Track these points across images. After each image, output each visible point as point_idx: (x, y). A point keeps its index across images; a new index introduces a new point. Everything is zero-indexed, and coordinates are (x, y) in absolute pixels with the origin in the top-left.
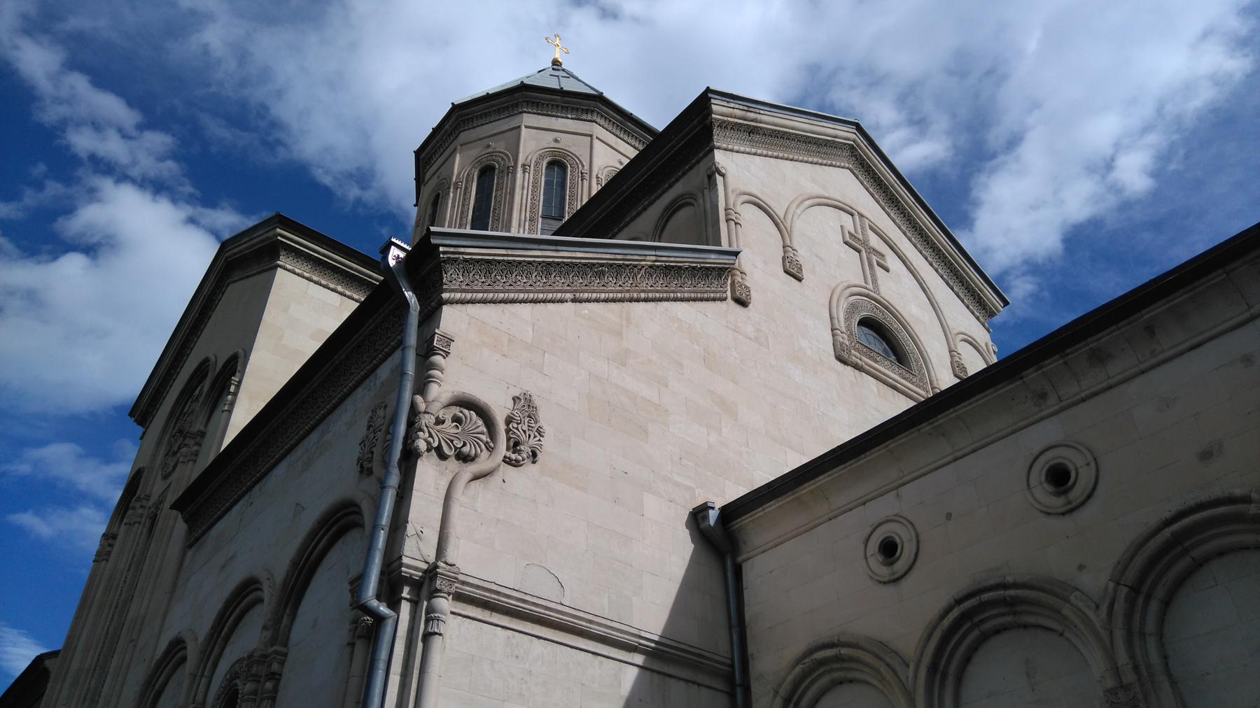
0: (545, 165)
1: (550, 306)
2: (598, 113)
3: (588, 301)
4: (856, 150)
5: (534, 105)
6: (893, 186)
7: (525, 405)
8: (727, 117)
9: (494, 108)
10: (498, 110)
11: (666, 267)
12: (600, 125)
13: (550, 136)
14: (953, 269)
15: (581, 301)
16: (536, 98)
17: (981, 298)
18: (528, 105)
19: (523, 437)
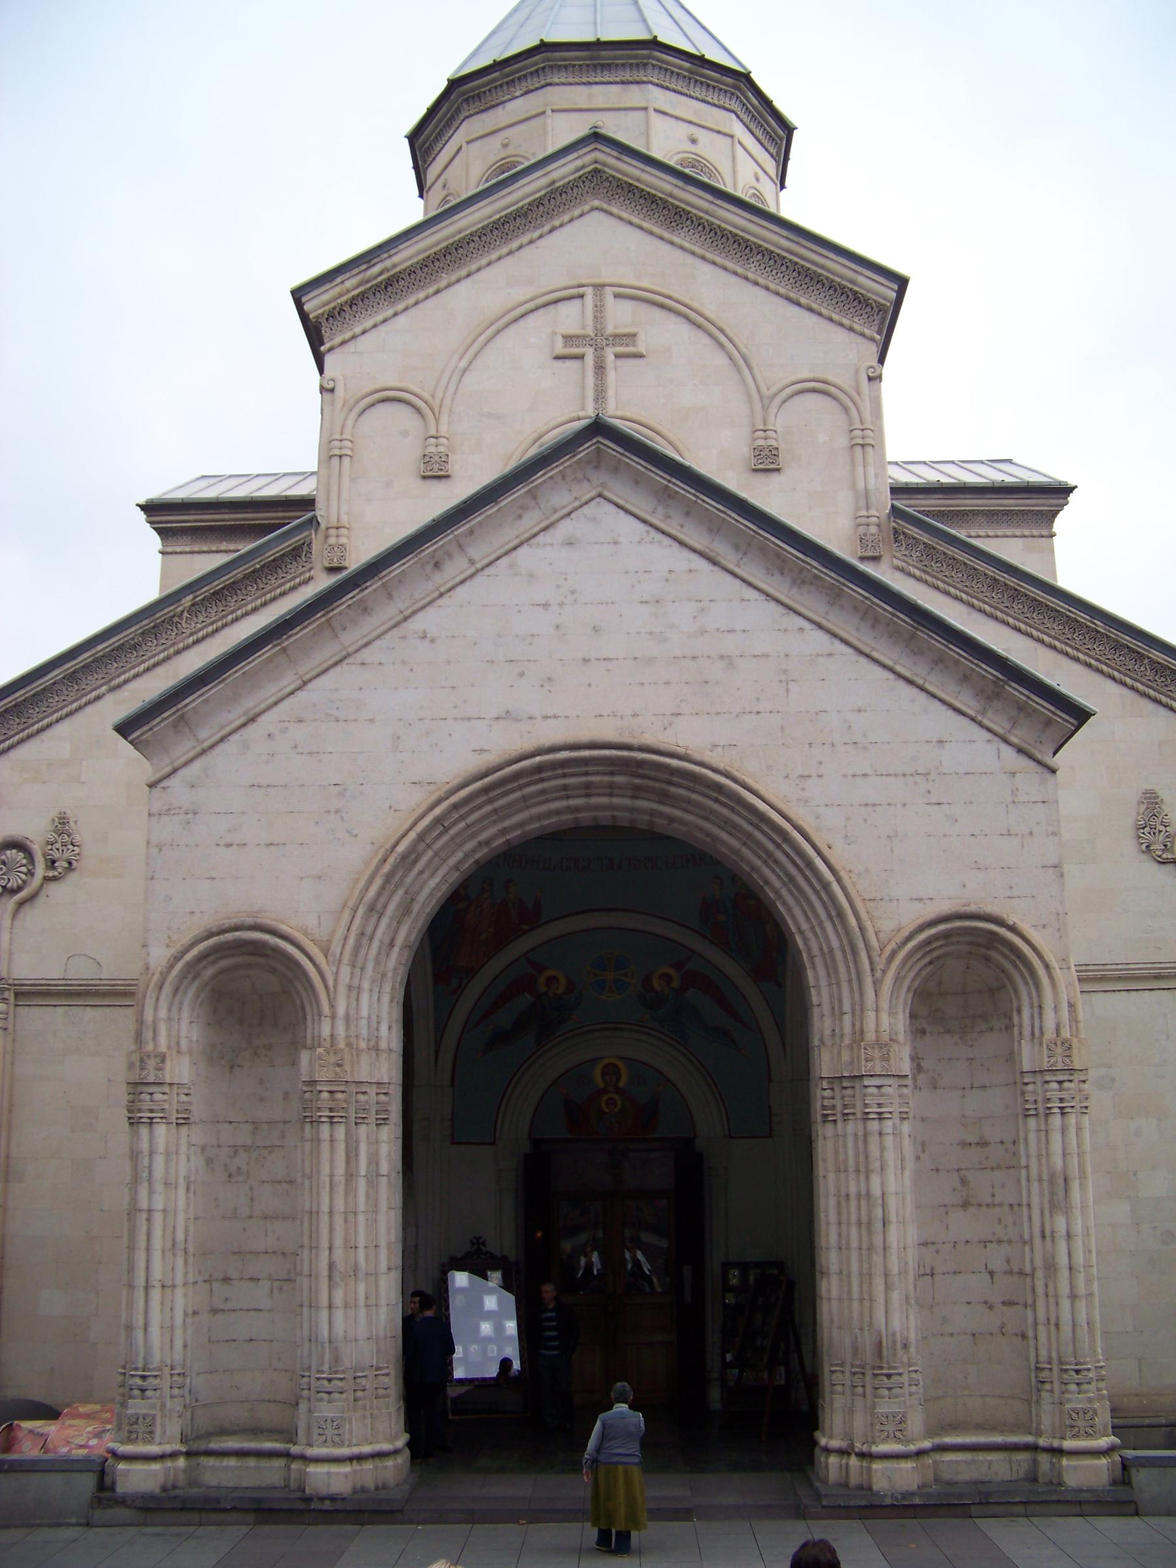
1: (89, 710)
2: (551, 67)
3: (126, 682)
4: (604, 172)
5: (476, 99)
6: (671, 195)
7: (62, 825)
8: (335, 299)
9: (443, 123)
10: (447, 123)
11: (213, 594)
12: (558, 84)
14: (801, 270)
15: (119, 686)
16: (473, 89)
17: (856, 293)
18: (468, 103)
19: (56, 855)
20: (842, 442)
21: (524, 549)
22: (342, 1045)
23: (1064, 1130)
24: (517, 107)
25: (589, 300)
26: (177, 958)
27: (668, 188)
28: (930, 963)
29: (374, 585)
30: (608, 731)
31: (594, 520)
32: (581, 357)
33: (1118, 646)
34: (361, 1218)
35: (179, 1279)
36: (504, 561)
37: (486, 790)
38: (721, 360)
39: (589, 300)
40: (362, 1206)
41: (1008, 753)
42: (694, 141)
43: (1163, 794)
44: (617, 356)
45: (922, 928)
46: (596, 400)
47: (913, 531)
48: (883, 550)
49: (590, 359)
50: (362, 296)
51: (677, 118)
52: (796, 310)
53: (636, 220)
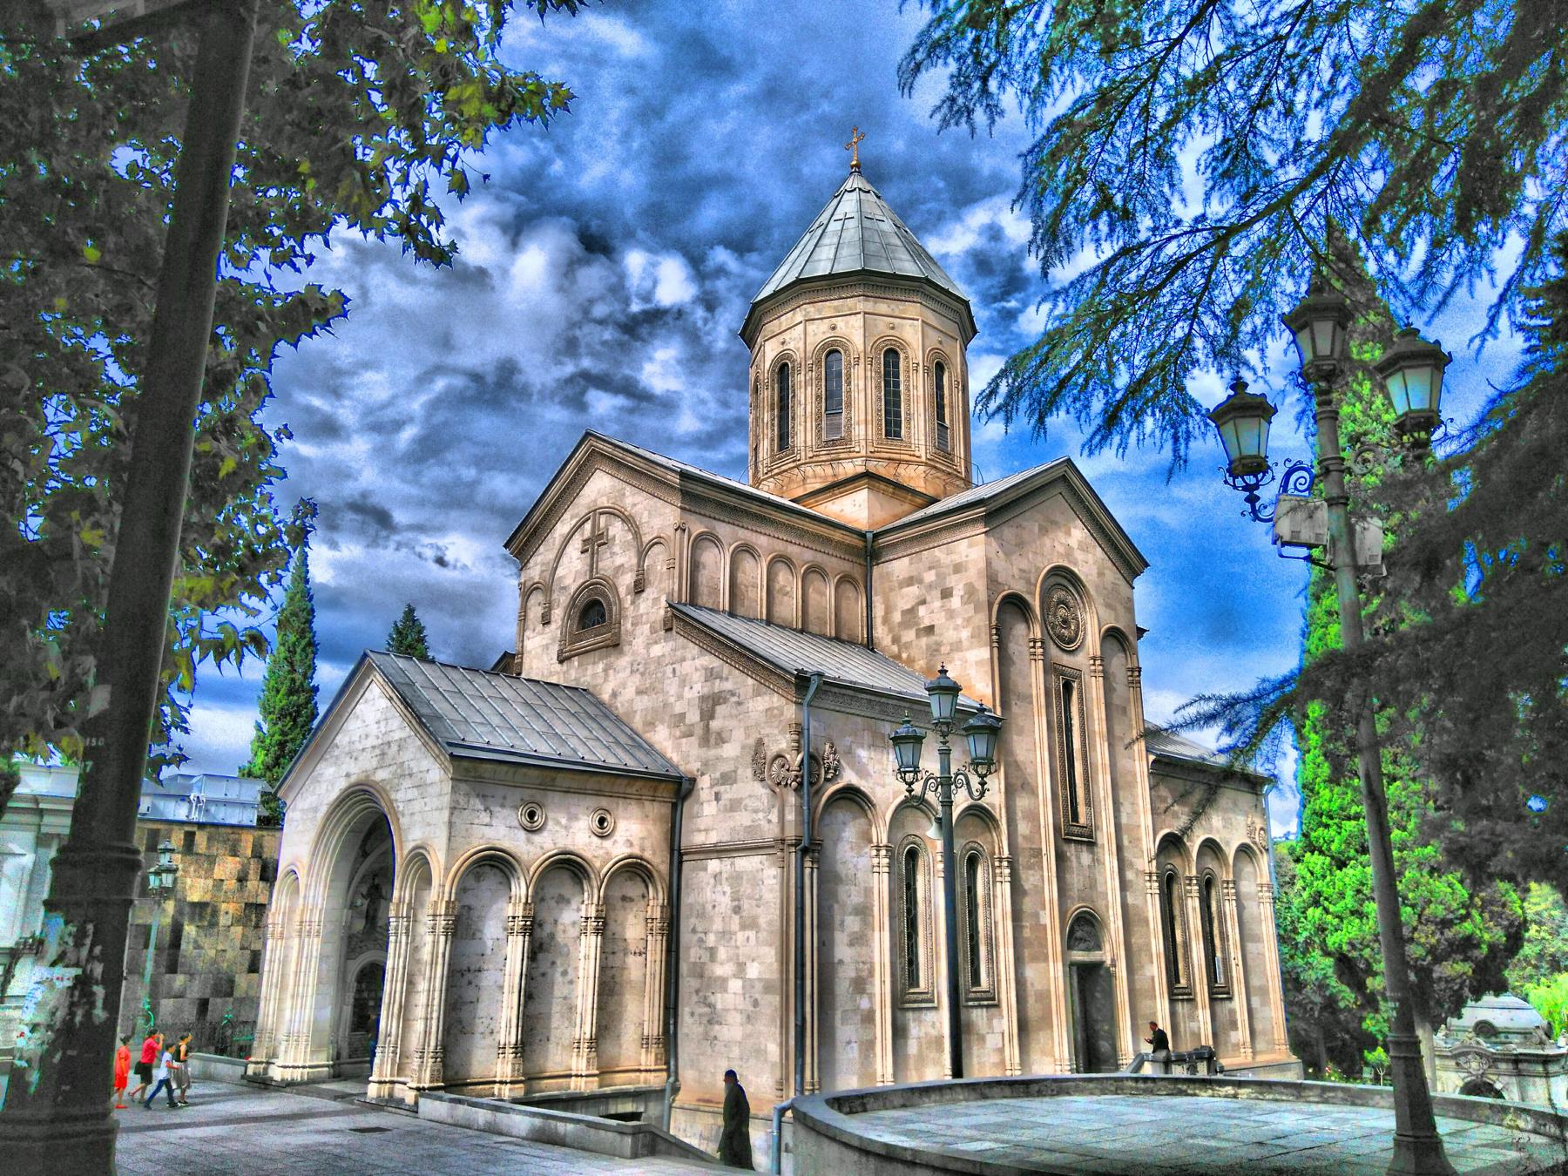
42: (834, 328)
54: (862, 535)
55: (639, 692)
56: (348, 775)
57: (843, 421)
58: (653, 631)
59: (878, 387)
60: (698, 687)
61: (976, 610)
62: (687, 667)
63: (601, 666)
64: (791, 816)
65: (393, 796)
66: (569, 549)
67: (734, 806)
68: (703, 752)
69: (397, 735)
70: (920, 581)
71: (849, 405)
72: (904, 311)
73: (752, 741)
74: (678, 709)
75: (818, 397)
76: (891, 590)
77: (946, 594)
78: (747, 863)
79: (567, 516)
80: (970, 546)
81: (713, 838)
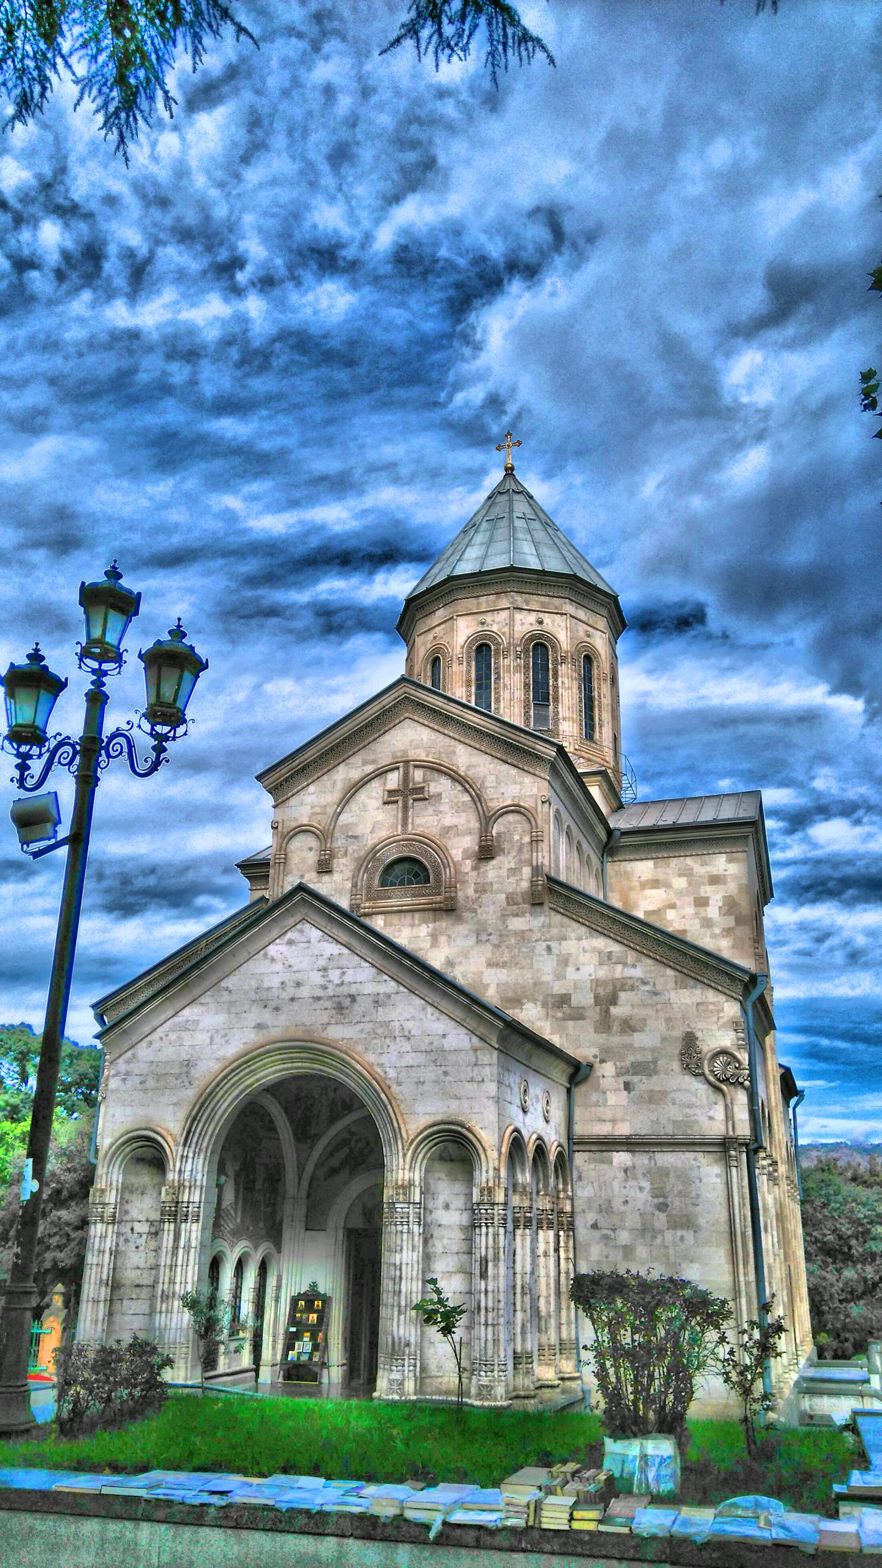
0: (429, 667)
13: (430, 636)
20: (527, 839)
21: (271, 947)
22: (176, 1184)
23: (487, 1234)
24: (440, 614)
25: (401, 769)
26: (112, 1144)
27: (440, 704)
28: (436, 1145)
29: (205, 967)
30: (299, 1034)
31: (301, 931)
32: (396, 802)
33: (672, 948)
34: (179, 1269)
35: (102, 1297)
36: (262, 953)
37: (246, 1062)
38: (466, 798)
39: (401, 769)
40: (179, 1263)
41: (475, 1040)
42: (541, 622)
43: (699, 1034)
44: (415, 800)
45: (426, 1129)
46: (402, 826)
47: (557, 888)
48: (546, 898)
49: (400, 803)
50: (291, 777)
51: (529, 610)
52: (506, 766)
53: (426, 723)
54: (610, 832)
55: (491, 964)
56: (259, 1027)
57: (551, 714)
58: (511, 900)
59: (580, 688)
60: (590, 969)
61: (739, 920)
62: (570, 946)
63: (424, 930)
64: (742, 1114)
65: (371, 1058)
66: (362, 796)
67: (654, 1098)
68: (602, 1038)
69: (370, 988)
70: (668, 886)
71: (556, 700)
72: (596, 622)
73: (678, 1032)
74: (558, 988)
75: (526, 685)
76: (631, 889)
77: (702, 902)
78: (666, 1159)
79: (357, 760)
80: (730, 861)
81: (624, 1129)
